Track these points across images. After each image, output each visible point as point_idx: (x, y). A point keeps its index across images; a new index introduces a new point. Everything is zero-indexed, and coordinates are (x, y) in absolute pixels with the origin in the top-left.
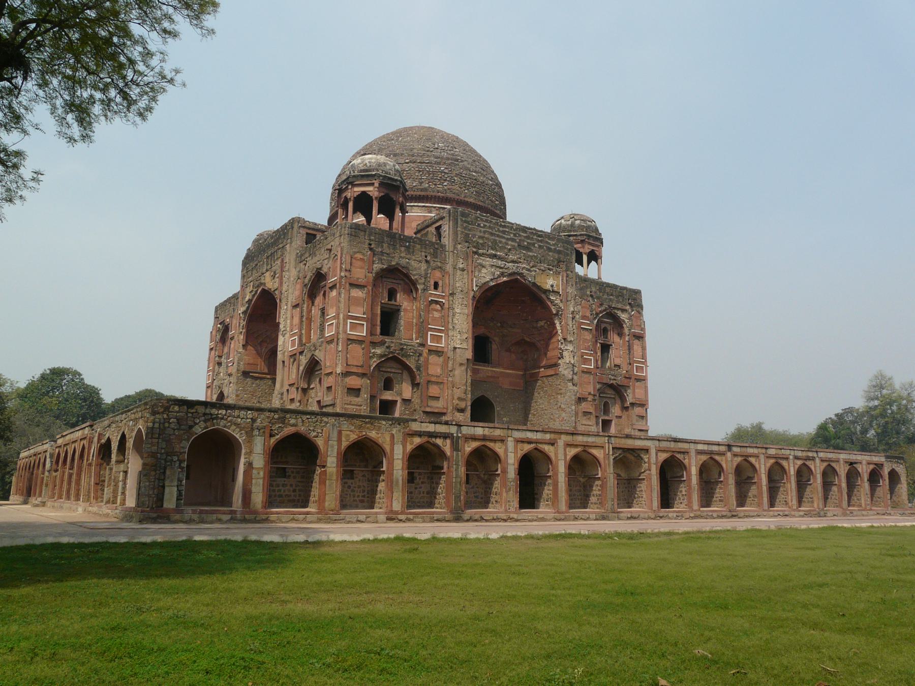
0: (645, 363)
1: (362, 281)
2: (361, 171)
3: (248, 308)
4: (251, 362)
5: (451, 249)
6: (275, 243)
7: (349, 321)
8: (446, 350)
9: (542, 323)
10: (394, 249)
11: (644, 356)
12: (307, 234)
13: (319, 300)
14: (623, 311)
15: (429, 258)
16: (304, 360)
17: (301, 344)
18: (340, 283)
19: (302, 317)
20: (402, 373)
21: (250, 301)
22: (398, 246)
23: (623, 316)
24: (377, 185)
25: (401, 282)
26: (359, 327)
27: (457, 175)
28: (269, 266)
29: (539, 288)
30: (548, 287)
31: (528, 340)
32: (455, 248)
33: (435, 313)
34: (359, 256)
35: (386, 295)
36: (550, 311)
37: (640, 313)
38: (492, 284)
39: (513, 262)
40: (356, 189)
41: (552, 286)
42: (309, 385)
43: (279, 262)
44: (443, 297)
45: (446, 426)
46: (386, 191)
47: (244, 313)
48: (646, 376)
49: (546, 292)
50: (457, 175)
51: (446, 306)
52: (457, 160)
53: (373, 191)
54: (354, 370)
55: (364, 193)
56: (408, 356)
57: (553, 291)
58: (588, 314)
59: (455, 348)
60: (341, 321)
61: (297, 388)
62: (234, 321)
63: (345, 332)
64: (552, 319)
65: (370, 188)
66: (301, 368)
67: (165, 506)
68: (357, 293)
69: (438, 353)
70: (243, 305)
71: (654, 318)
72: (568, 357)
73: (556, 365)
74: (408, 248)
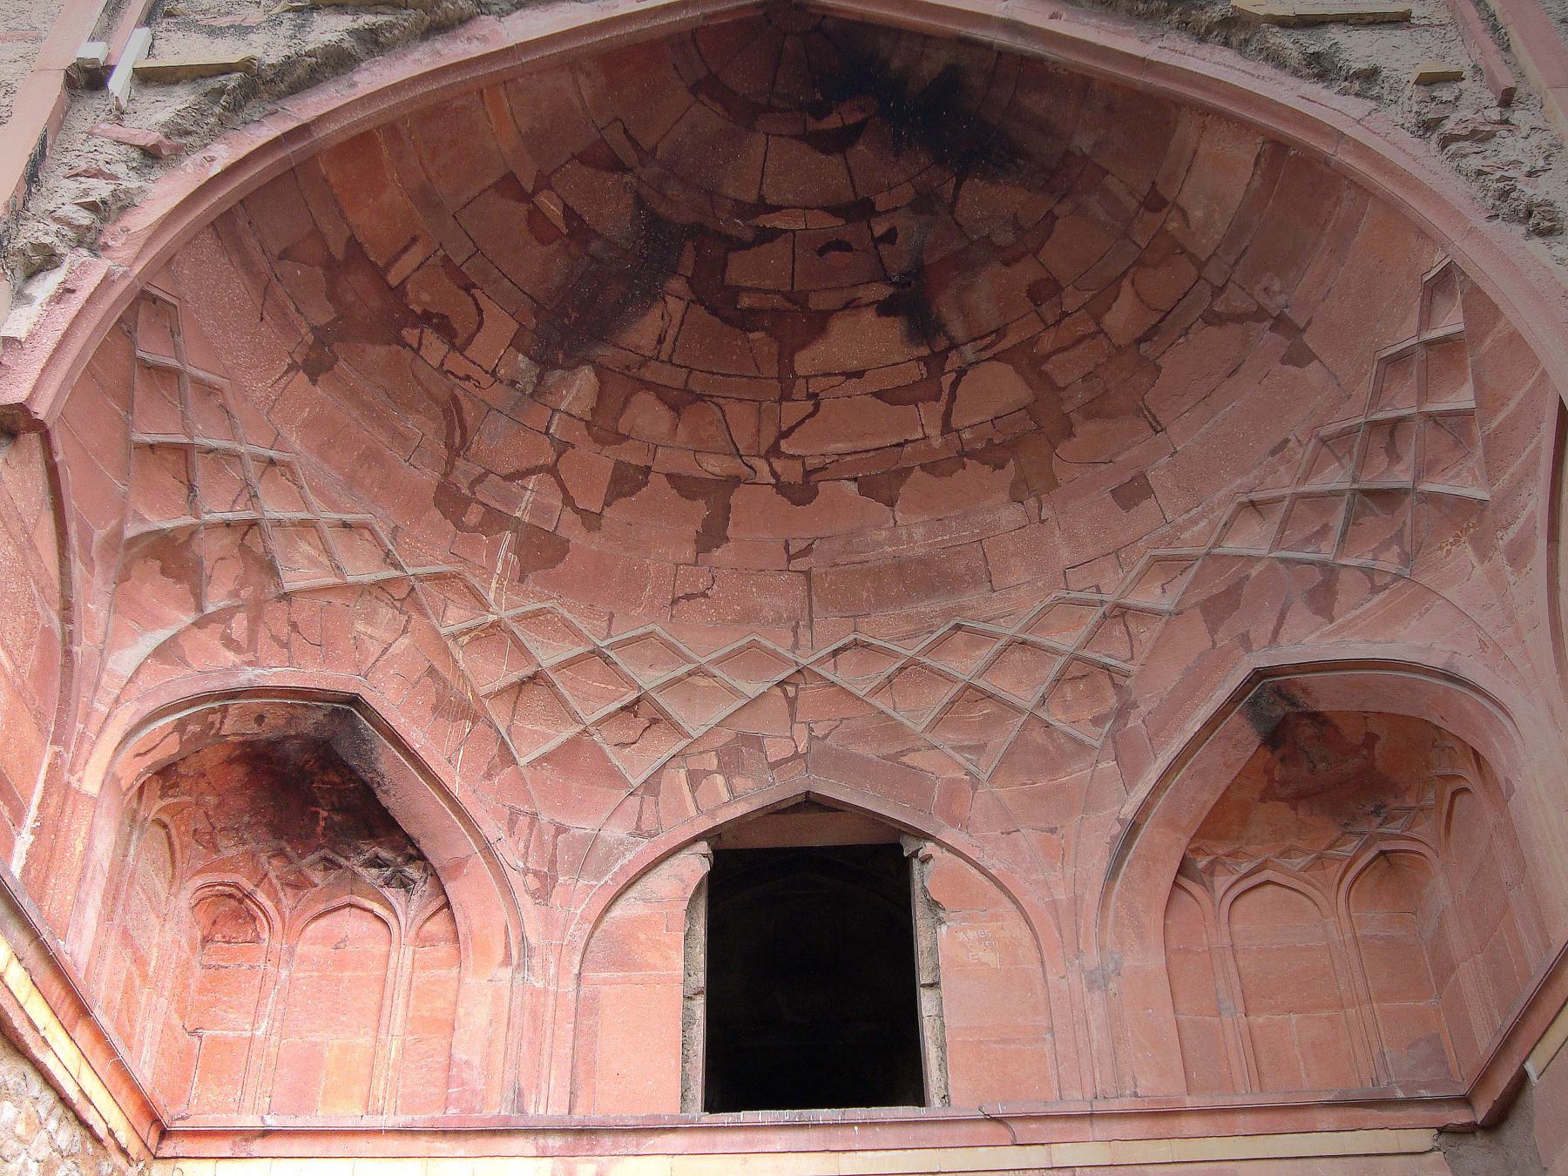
3: (336, 62)
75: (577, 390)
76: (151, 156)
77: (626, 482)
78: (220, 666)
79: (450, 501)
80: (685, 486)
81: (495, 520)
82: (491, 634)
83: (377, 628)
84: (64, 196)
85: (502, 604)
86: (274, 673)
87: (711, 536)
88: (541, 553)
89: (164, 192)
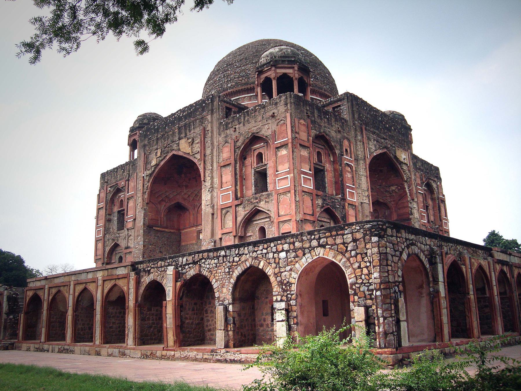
0: (447, 220)
1: (307, 144)
2: (281, 57)
3: (154, 171)
4: (154, 217)
5: (352, 124)
6: (189, 115)
7: (302, 175)
8: (357, 204)
9: (393, 188)
10: (321, 119)
11: (446, 216)
12: (227, 108)
13: (251, 160)
14: (434, 181)
15: (340, 129)
16: (242, 213)
17: (237, 198)
18: (292, 143)
19: (236, 174)
20: (330, 223)
21: (157, 165)
22: (323, 117)
23: (434, 185)
24: (296, 68)
25: (323, 147)
26: (308, 181)
27: (318, 74)
28: (183, 135)
29: (397, 159)
30: (402, 160)
31: (381, 201)
32: (354, 124)
33: (348, 174)
34: (302, 121)
35: (316, 157)
36: (402, 178)
37: (441, 183)
38: (375, 154)
39: (384, 138)
40: (278, 71)
41: (404, 159)
42: (245, 234)
43: (198, 130)
44: (351, 162)
45: (508, 257)
46: (301, 75)
47: (151, 175)
48: (448, 230)
49: (401, 163)
50: (318, 74)
51: (354, 169)
52: (316, 64)
53: (293, 72)
54: (308, 218)
55: (285, 74)
56: (336, 208)
57: (405, 164)
58: (420, 182)
59: (362, 203)
60: (296, 175)
61: (235, 237)
62: (132, 184)
63: (301, 185)
64: (403, 185)
65: (290, 71)
66: (239, 219)
67: (403, 345)
68: (305, 153)
69: (351, 205)
70: (146, 169)
71: (449, 187)
72: (416, 215)
73: (410, 219)
74: (328, 119)
75: (183, 175)
76: (148, 182)
77: (190, 180)
78: (168, 205)
79: (179, 186)
80: (194, 178)
81: (183, 186)
82: (185, 194)
83: (178, 197)
84: (145, 188)
85: (185, 191)
86: (173, 203)
87: (196, 181)
88: (187, 187)
89: (150, 184)
